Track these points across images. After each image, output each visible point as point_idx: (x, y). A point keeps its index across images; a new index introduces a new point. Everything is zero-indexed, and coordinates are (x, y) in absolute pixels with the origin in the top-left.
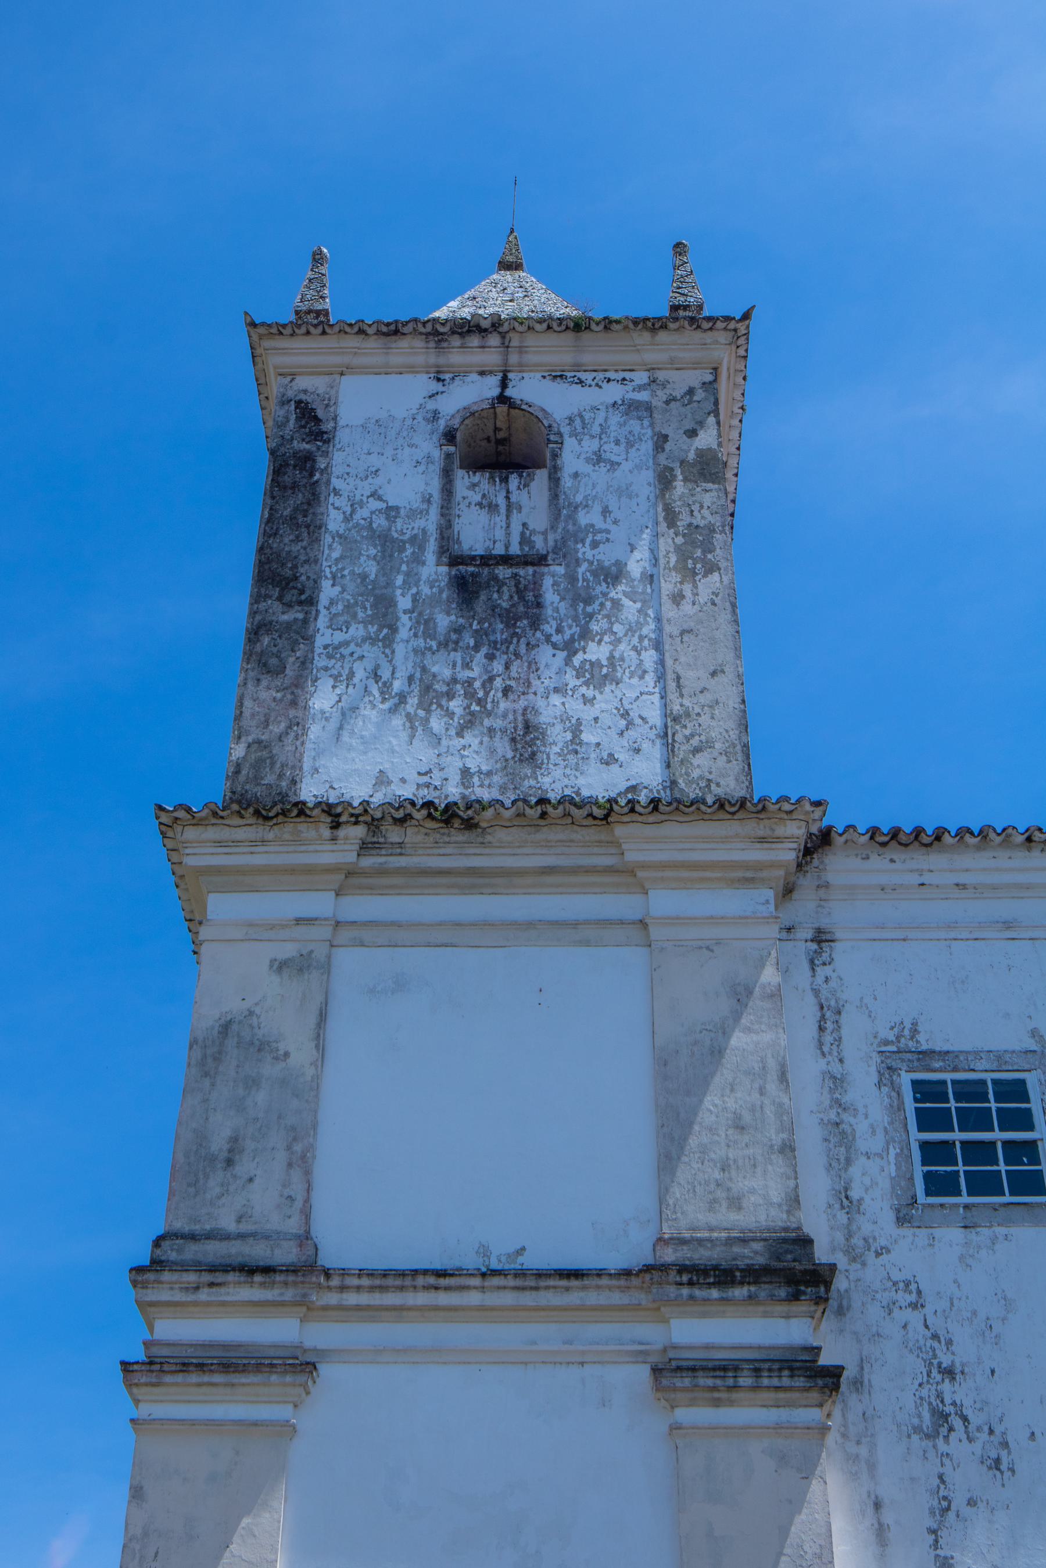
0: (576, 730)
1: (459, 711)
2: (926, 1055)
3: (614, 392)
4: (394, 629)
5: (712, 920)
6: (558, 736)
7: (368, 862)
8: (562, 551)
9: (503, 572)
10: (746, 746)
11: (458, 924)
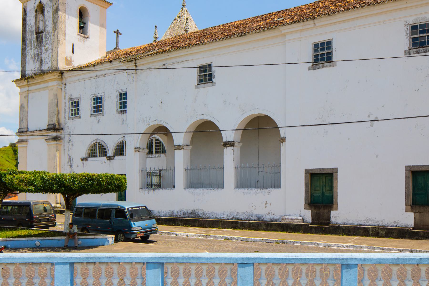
0: (45, 60)
1: (37, 59)
4: (32, 46)
5: (52, 86)
6: (44, 61)
7: (28, 83)
8: (45, 30)
9: (40, 35)
10: (57, 59)
11: (36, 89)
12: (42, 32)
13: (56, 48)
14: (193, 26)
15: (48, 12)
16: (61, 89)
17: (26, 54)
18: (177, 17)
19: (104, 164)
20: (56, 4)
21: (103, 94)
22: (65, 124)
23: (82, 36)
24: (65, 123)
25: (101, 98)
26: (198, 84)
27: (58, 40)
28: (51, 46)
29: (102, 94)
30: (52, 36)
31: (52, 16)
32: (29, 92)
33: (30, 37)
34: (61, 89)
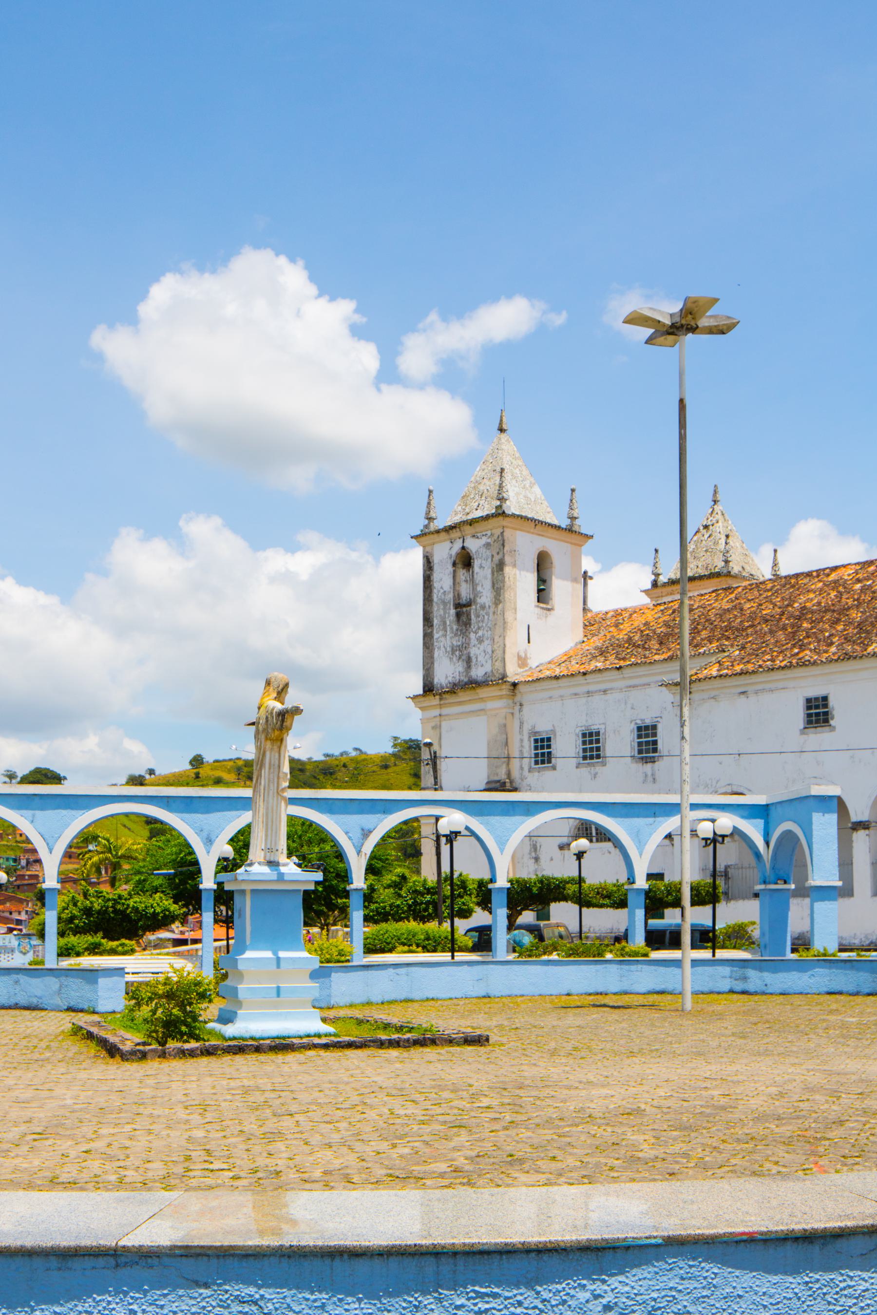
2: (536, 733)
3: (484, 540)
5: (496, 709)
6: (474, 660)
7: (442, 702)
8: (475, 601)
9: (464, 609)
12: (469, 604)
13: (502, 638)
14: (738, 544)
15: (481, 567)
16: (512, 714)
17: (433, 644)
18: (701, 528)
19: (607, 854)
20: (498, 553)
21: (603, 727)
22: (522, 780)
23: (543, 608)
24: (523, 779)
25: (598, 733)
26: (805, 728)
27: (505, 623)
28: (489, 632)
29: (600, 727)
30: (491, 614)
31: (489, 576)
32: (443, 718)
33: (442, 612)
34: (512, 714)
